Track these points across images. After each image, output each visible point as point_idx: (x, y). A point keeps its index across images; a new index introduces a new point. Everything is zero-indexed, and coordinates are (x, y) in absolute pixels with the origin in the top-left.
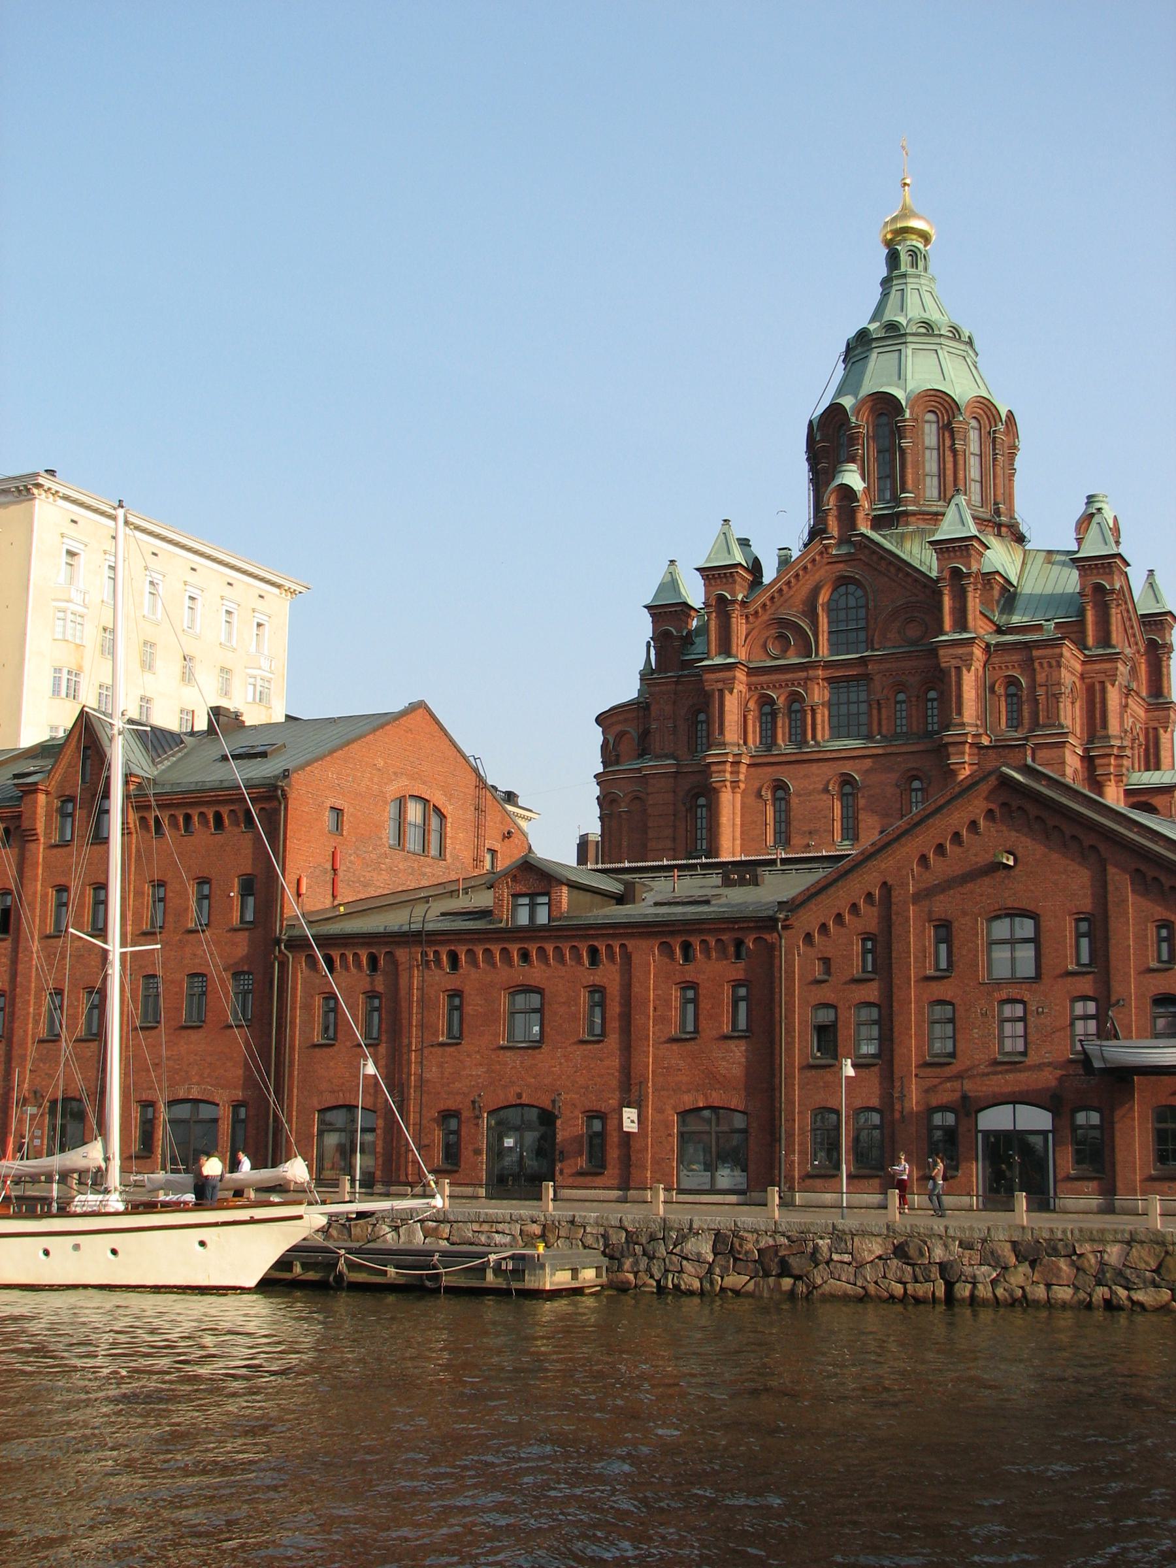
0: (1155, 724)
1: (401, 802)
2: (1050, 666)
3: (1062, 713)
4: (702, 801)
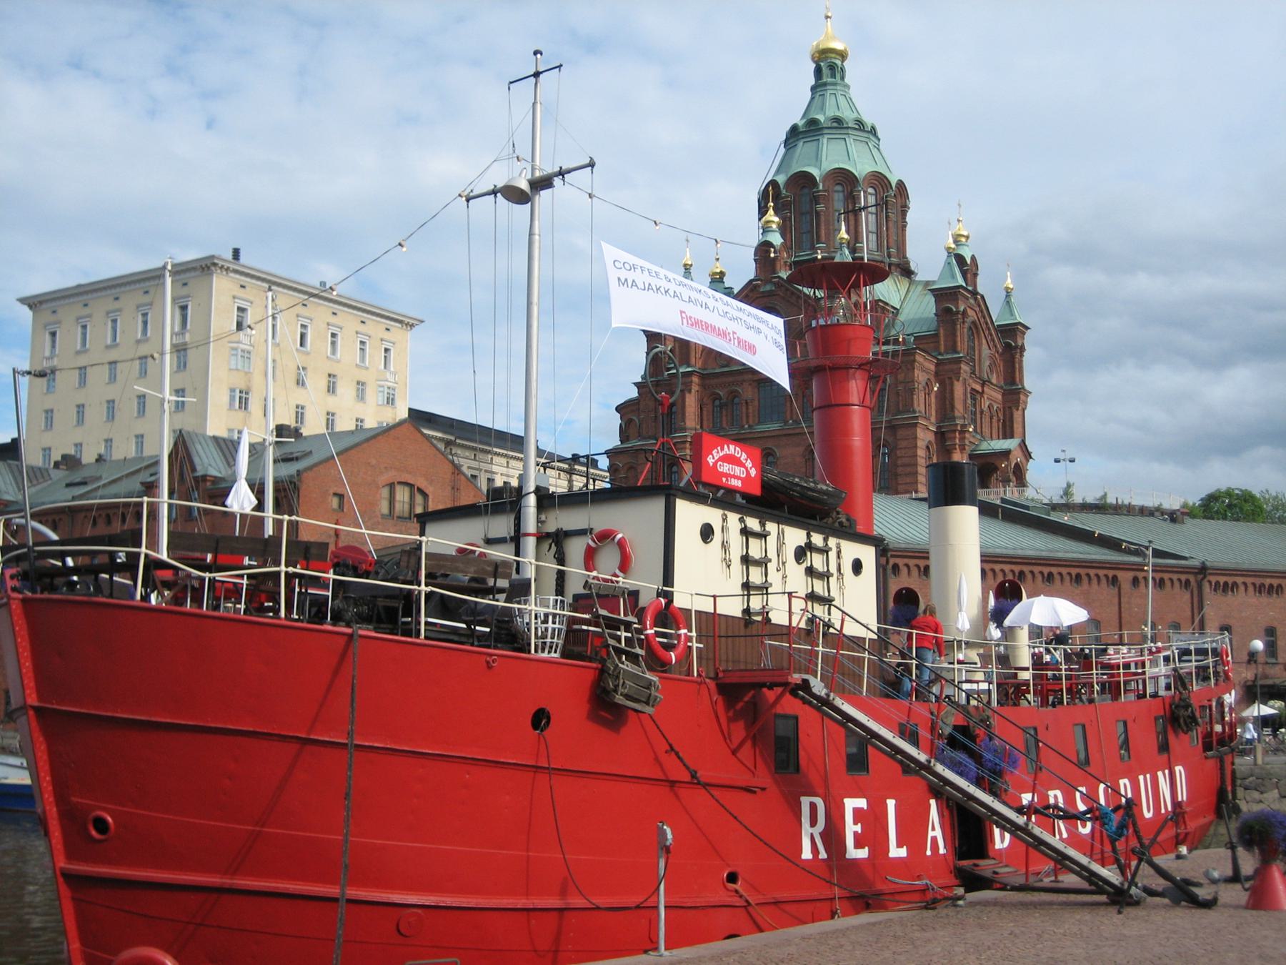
0: (1008, 404)
1: (392, 486)
2: (908, 369)
3: (915, 402)
4: (675, 469)
